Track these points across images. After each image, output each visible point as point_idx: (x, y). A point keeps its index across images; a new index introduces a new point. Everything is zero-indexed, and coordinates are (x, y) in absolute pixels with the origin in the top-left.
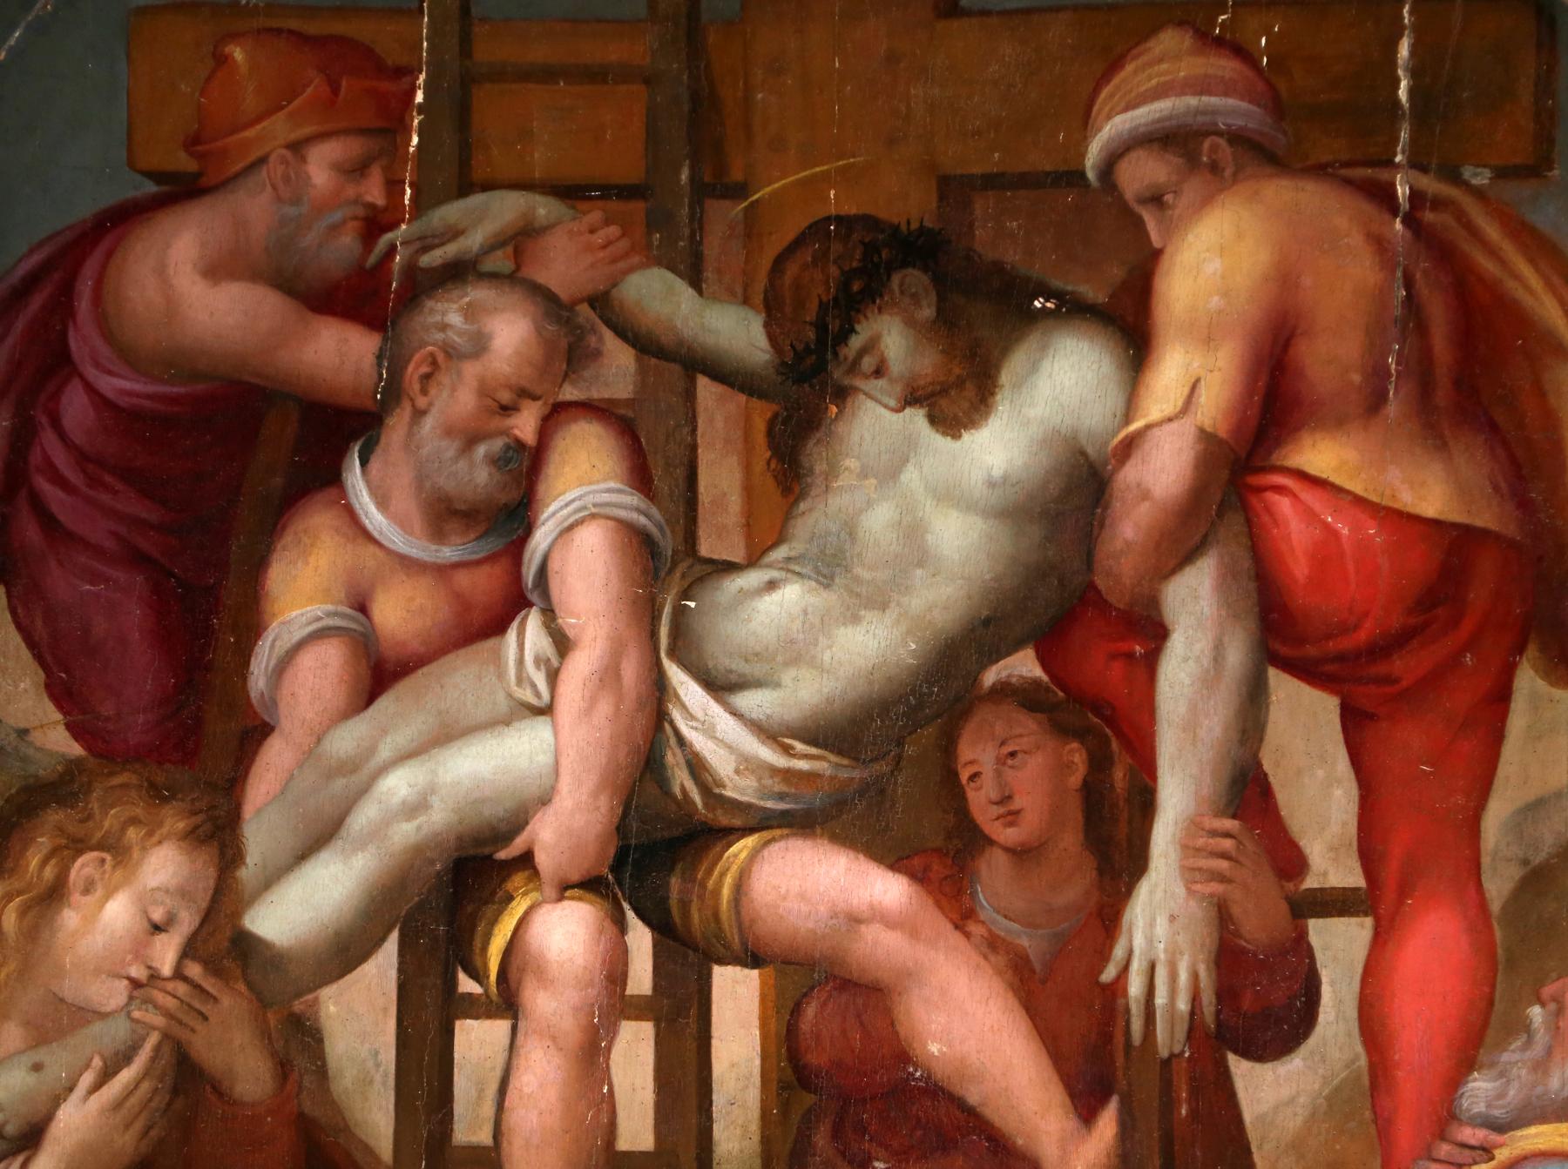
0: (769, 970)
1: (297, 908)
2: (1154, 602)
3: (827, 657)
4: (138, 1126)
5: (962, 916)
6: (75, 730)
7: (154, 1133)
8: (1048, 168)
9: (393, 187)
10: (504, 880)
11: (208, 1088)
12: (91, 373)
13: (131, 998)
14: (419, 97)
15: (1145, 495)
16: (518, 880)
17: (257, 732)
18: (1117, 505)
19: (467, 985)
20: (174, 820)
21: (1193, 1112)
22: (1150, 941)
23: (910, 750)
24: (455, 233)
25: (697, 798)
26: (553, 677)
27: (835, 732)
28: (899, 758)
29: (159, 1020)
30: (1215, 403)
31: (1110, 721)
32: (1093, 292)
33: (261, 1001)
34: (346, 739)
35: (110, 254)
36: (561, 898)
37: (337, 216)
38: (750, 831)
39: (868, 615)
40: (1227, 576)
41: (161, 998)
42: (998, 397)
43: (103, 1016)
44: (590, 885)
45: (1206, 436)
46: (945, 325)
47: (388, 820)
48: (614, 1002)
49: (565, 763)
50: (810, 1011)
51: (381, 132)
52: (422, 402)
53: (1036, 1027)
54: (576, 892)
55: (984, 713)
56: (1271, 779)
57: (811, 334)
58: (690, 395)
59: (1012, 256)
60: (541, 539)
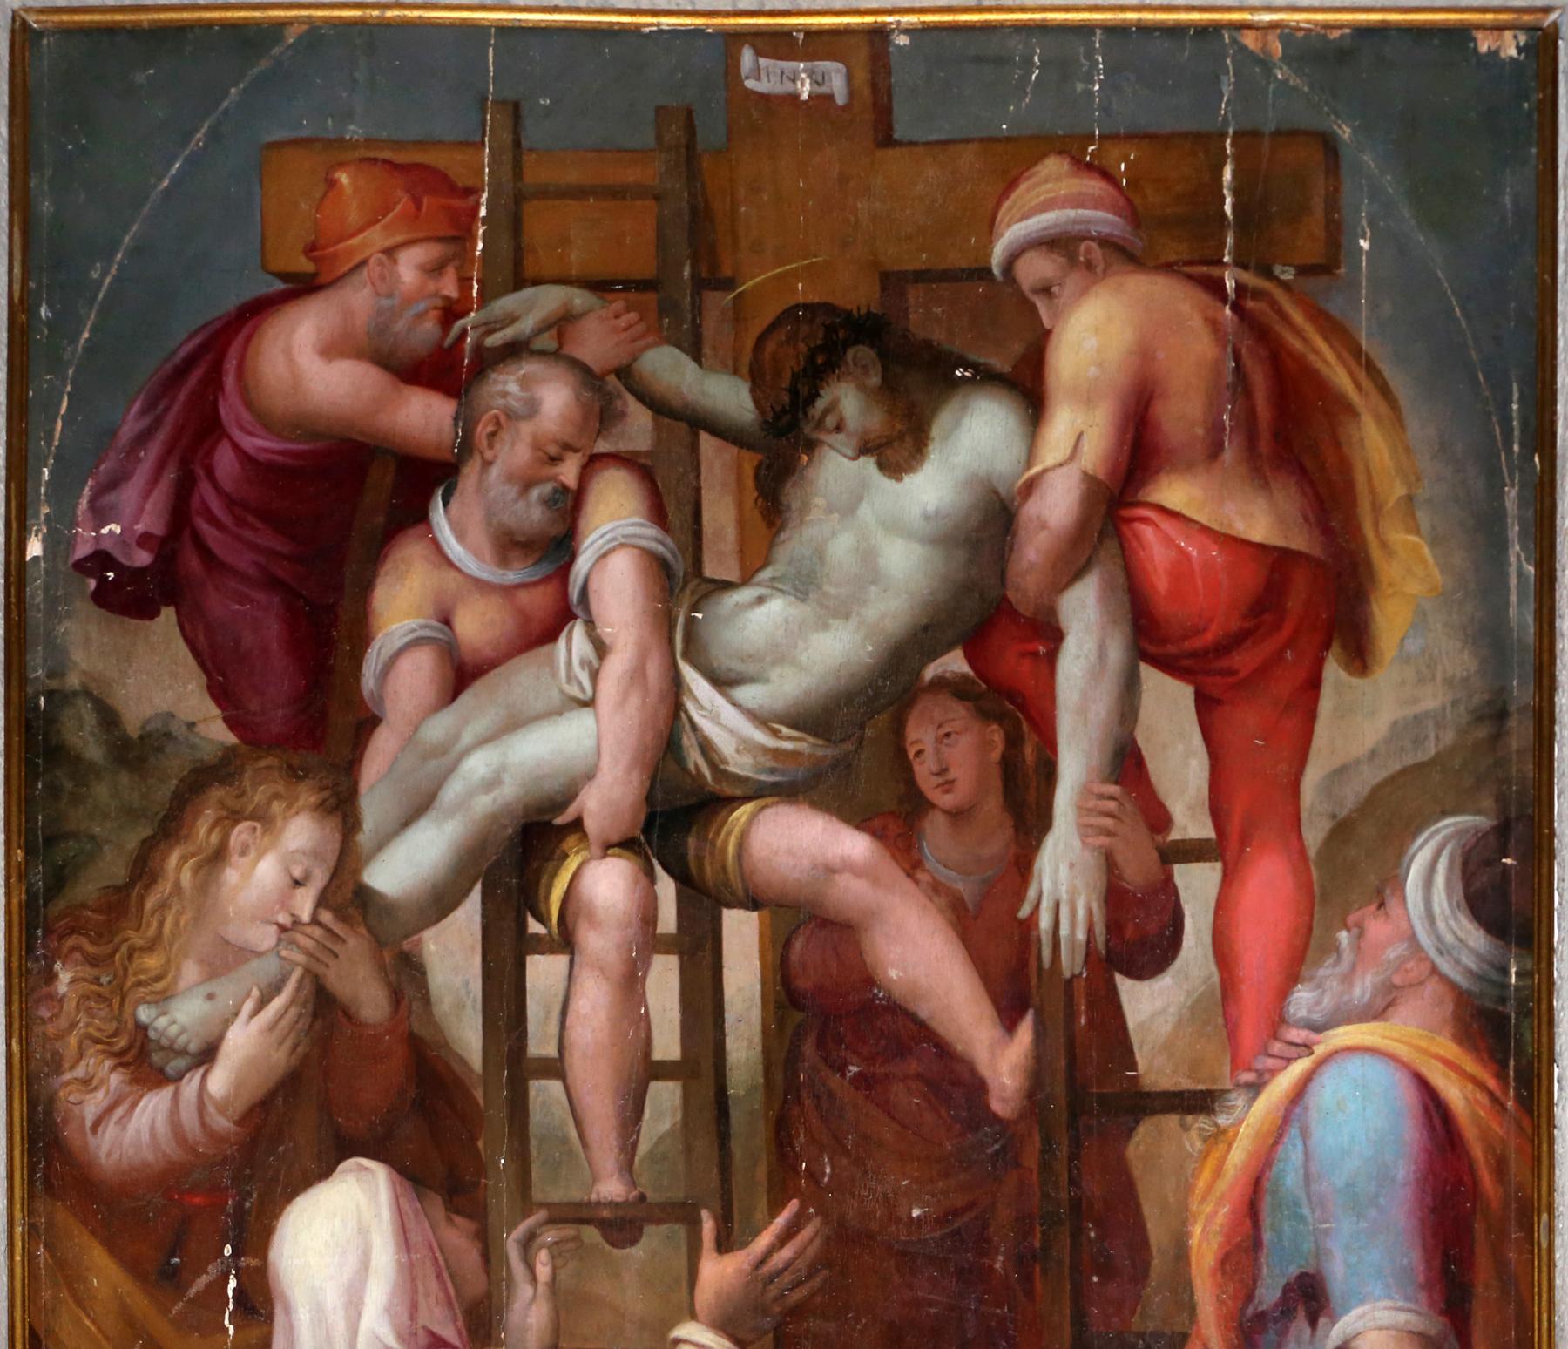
0: (766, 912)
1: (403, 866)
2: (1052, 611)
3: (804, 658)
4: (288, 1043)
6: (232, 723)
7: (300, 1049)
8: (964, 265)
9: (464, 283)
10: (561, 841)
11: (340, 1014)
12: (237, 435)
13: (279, 940)
14: (483, 212)
15: (1043, 526)
16: (571, 841)
17: (369, 723)
18: (1022, 533)
19: (534, 927)
20: (308, 796)
21: (1090, 1022)
22: (1055, 883)
23: (869, 732)
24: (512, 319)
25: (707, 772)
26: (595, 676)
27: (813, 719)
28: (861, 739)
29: (300, 958)
31: (1022, 707)
32: (1000, 363)
33: (378, 942)
34: (437, 728)
35: (248, 339)
36: (605, 855)
37: (422, 306)
38: (747, 799)
39: (834, 623)
40: (1107, 589)
41: (301, 939)
42: (931, 448)
43: (259, 954)
44: (627, 845)
45: (1089, 479)
46: (889, 391)
47: (470, 794)
48: (648, 941)
49: (604, 745)
50: (798, 945)
51: (454, 239)
52: (489, 455)
53: (970, 955)
54: (616, 850)
55: (925, 702)
56: (1144, 752)
57: (786, 398)
58: (694, 447)
59: (938, 336)
60: (582, 564)
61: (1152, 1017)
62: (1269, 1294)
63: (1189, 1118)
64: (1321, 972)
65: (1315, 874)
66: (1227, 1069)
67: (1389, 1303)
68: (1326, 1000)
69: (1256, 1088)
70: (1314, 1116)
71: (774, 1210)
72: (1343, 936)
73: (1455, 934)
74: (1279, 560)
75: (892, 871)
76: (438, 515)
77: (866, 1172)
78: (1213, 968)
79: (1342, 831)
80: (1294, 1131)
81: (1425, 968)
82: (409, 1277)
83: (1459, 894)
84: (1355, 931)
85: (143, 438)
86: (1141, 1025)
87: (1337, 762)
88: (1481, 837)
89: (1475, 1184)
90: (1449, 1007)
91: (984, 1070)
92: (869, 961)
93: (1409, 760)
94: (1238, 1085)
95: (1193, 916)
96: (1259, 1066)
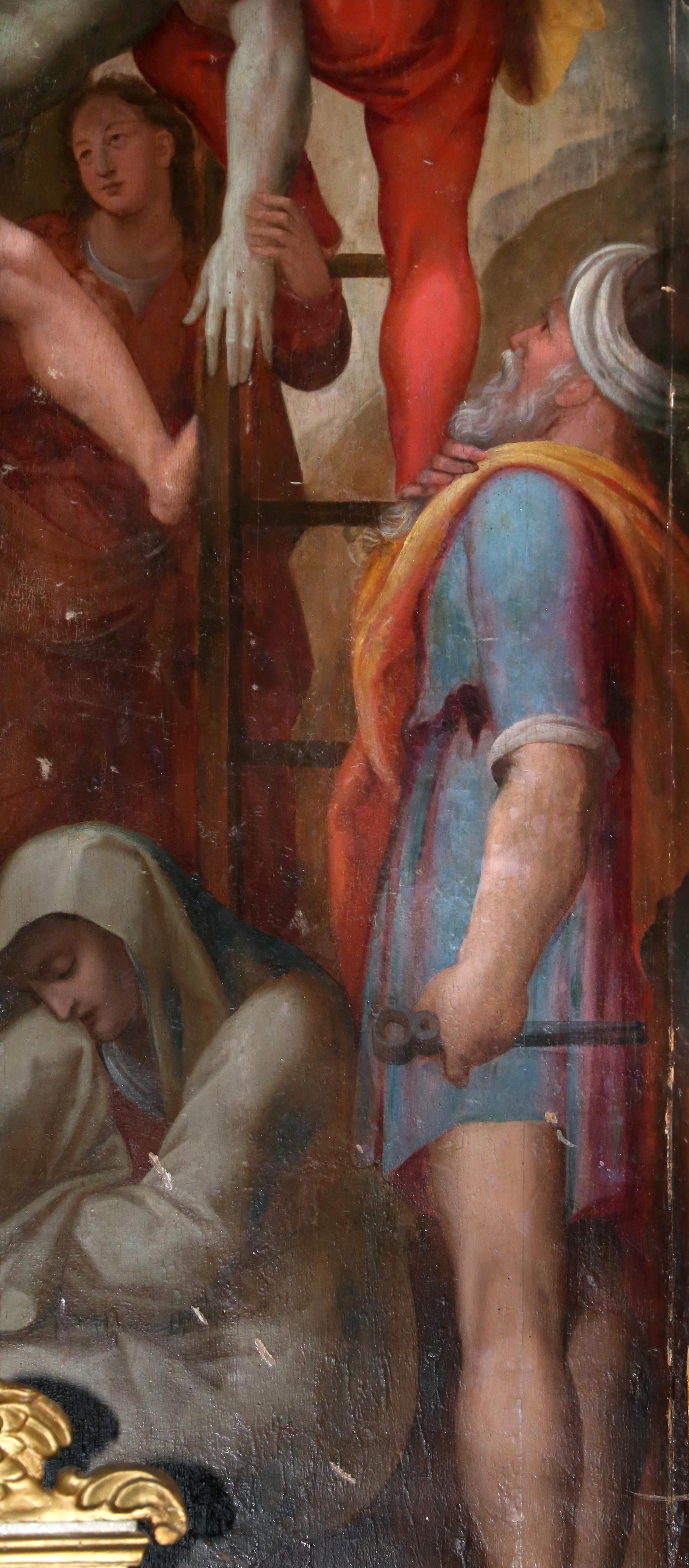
2: (225, 22)
5: (76, 266)
21: (256, 431)
22: (222, 291)
23: (34, 129)
31: (191, 115)
53: (134, 358)
56: (314, 166)
61: (318, 428)
62: (431, 705)
63: (354, 530)
64: (487, 390)
65: (481, 295)
66: (392, 482)
67: (550, 717)
68: (491, 418)
69: (421, 502)
70: (478, 533)
72: (508, 355)
73: (616, 357)
75: (55, 271)
77: (18, 573)
78: (380, 382)
79: (508, 253)
80: (457, 545)
81: (588, 389)
83: (620, 318)
84: (520, 351)
86: (306, 436)
87: (503, 186)
88: (642, 265)
89: (635, 599)
90: (611, 429)
91: (146, 475)
92: (27, 358)
93: (573, 187)
94: (403, 498)
95: (360, 330)
96: (424, 480)
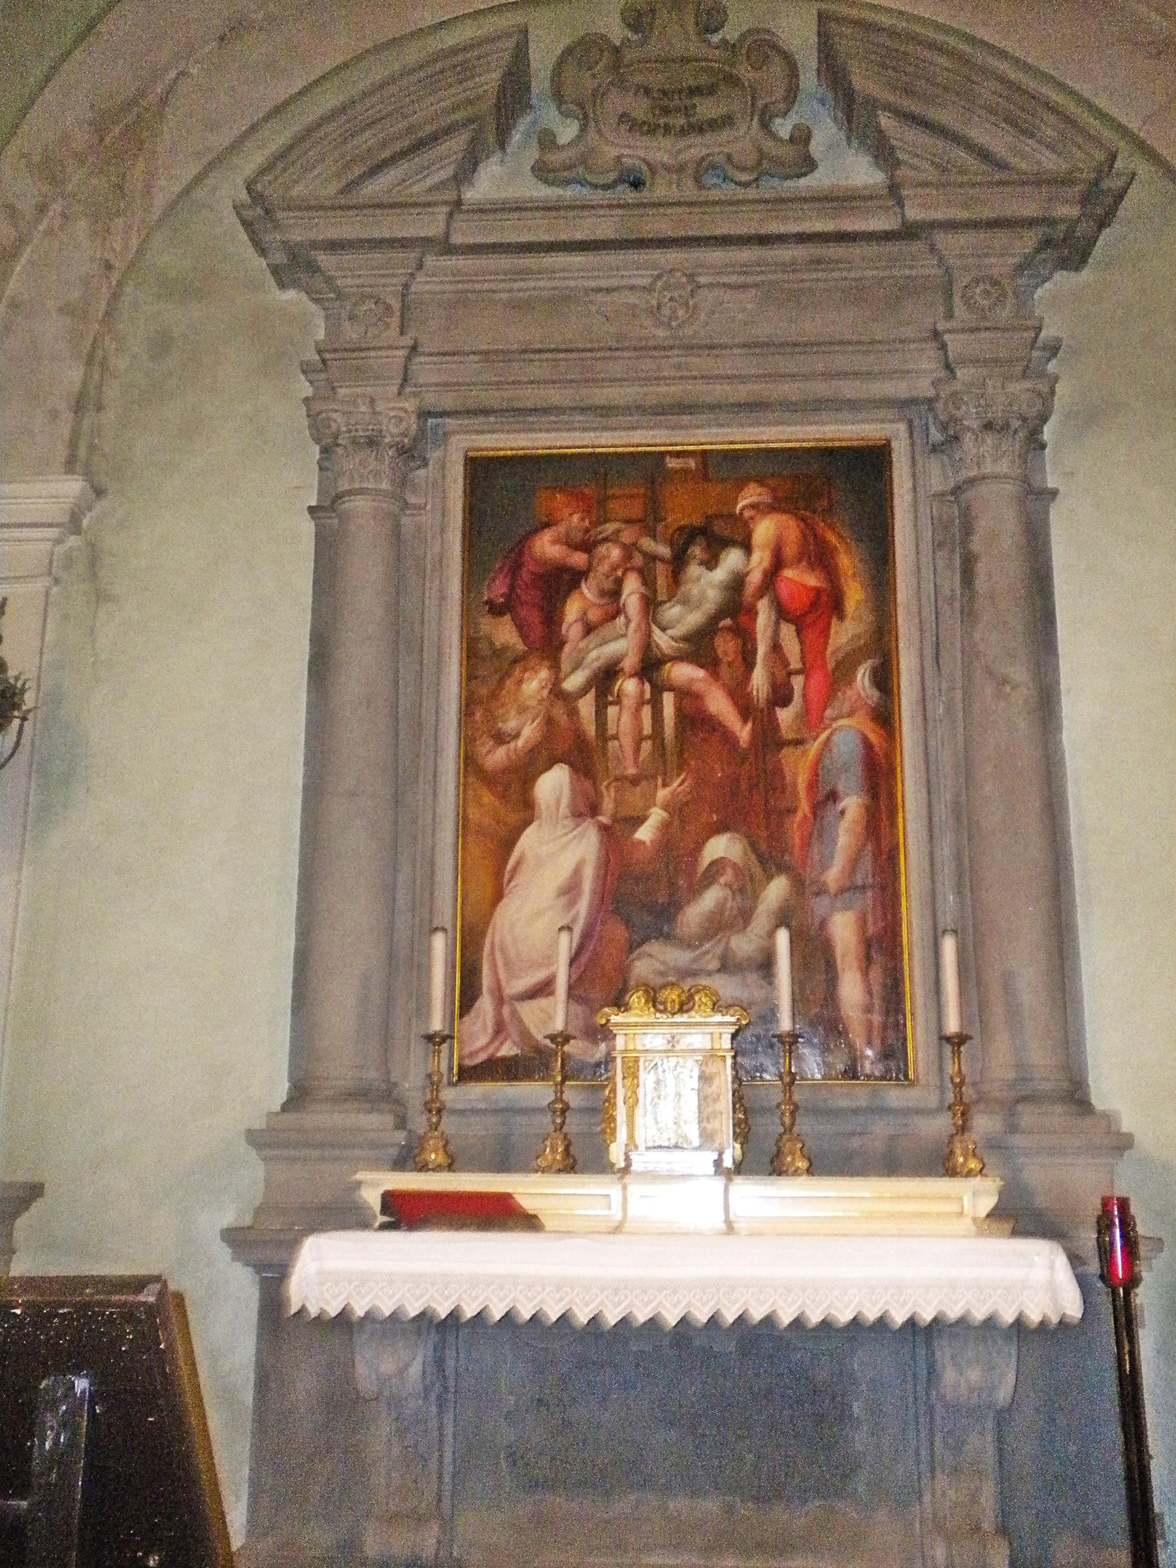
17: (562, 643)
20: (546, 663)
27: (685, 639)
30: (766, 563)
34: (582, 645)
46: (709, 547)
48: (641, 703)
60: (623, 597)
62: (820, 797)
71: (678, 776)
74: (818, 591)
76: (583, 585)
79: (838, 664)
82: (573, 799)
85: (501, 569)
91: (738, 734)
